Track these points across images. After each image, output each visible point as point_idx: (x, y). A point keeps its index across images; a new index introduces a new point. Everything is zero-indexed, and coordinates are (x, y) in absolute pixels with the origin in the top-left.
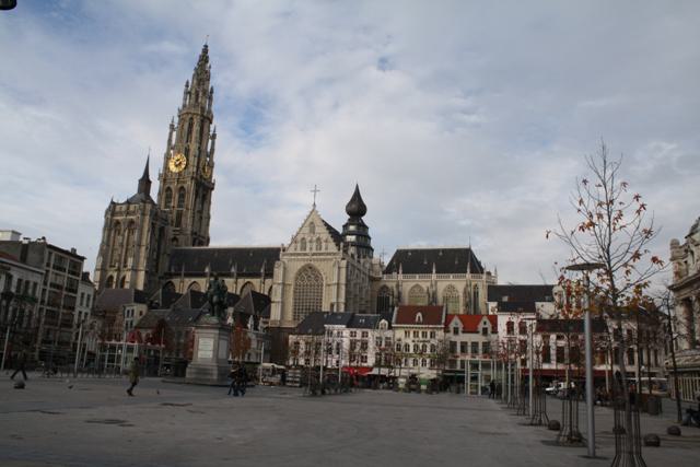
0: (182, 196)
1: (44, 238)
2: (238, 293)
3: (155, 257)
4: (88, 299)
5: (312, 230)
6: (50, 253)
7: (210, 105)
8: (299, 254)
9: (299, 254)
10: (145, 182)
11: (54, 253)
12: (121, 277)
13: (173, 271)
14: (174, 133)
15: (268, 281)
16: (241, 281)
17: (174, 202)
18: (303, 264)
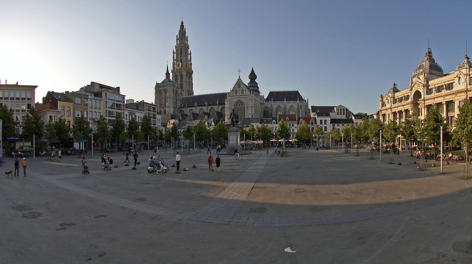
0: (182, 78)
1: (143, 100)
2: (209, 112)
3: (175, 102)
4: (160, 120)
5: (239, 87)
6: (146, 105)
7: (187, 42)
8: (234, 96)
9: (234, 96)
10: (168, 74)
11: (147, 105)
12: (164, 110)
13: (182, 106)
14: (175, 55)
15: (221, 107)
16: (209, 107)
17: (179, 80)
18: (236, 99)
